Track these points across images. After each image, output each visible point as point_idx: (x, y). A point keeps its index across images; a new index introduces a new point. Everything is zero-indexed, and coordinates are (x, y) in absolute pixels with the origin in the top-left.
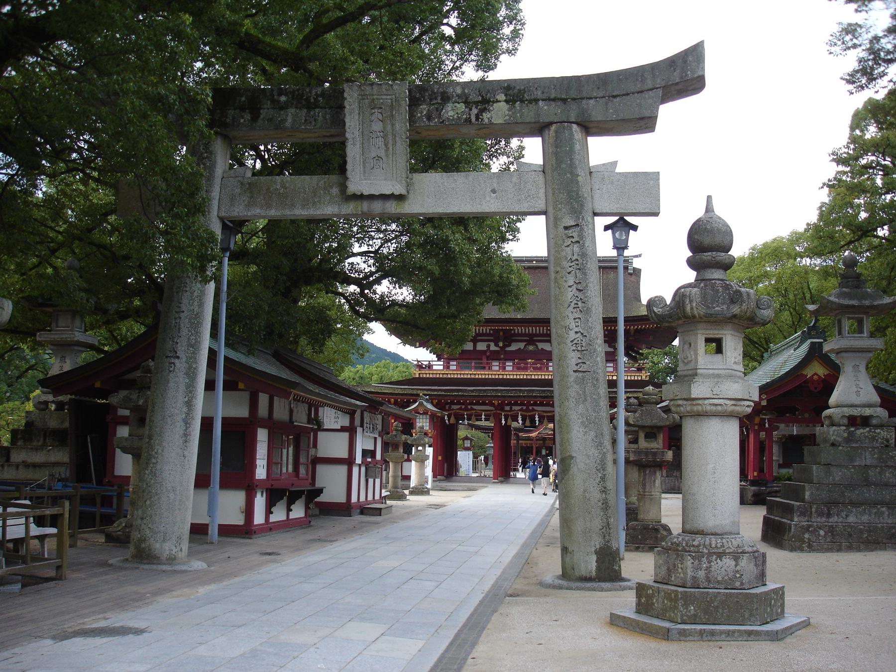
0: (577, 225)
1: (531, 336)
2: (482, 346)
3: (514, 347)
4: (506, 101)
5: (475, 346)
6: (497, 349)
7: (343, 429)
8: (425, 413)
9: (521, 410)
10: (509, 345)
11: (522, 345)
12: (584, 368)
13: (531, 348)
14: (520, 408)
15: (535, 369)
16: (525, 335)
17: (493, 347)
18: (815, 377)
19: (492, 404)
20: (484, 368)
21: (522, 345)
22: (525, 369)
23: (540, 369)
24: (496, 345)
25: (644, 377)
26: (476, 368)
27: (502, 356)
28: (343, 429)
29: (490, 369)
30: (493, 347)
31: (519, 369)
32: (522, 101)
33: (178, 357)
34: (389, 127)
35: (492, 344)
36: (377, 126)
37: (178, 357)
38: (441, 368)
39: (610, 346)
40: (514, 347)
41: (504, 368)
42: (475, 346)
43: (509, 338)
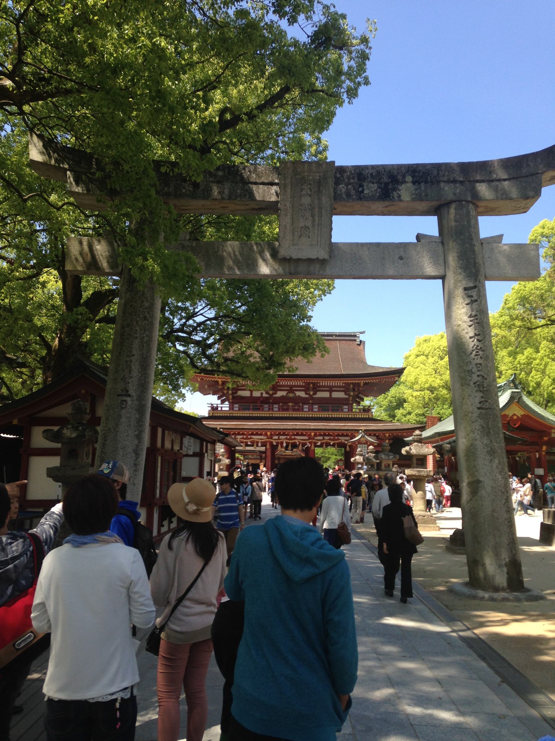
0: (475, 287)
1: (291, 387)
4: (414, 183)
6: (267, 396)
7: (195, 455)
9: (286, 439)
10: (276, 393)
11: (284, 393)
12: (487, 405)
13: (291, 395)
14: (285, 437)
15: (294, 410)
18: (515, 417)
19: (266, 434)
22: (287, 410)
23: (298, 410)
26: (255, 409)
28: (195, 455)
29: (263, 410)
31: (284, 410)
32: (426, 182)
33: (129, 396)
34: (316, 202)
36: (306, 200)
37: (129, 396)
38: (228, 409)
39: (346, 394)
40: (280, 394)
41: (273, 409)
43: (275, 388)
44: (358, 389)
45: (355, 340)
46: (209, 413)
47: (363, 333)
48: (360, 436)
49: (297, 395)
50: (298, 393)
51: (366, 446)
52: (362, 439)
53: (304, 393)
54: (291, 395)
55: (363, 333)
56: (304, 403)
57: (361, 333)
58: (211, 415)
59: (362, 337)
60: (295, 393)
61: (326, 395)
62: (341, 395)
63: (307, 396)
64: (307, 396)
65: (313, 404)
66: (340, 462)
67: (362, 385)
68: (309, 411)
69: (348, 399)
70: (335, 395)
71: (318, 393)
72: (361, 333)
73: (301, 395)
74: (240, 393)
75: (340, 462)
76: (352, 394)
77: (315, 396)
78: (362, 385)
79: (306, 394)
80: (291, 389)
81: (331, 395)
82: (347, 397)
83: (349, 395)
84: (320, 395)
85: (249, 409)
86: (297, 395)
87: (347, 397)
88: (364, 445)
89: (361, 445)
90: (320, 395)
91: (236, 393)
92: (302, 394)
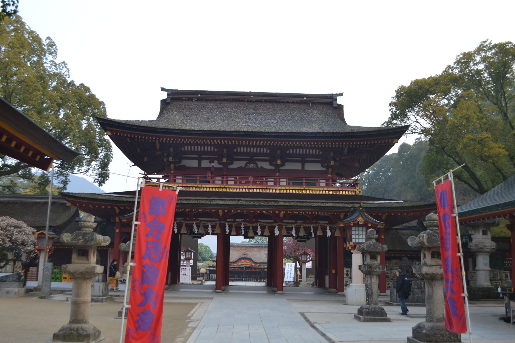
2: (205, 164)
3: (236, 165)
5: (200, 164)
10: (232, 164)
11: (243, 164)
13: (251, 166)
16: (247, 154)
20: (208, 182)
21: (243, 164)
22: (248, 183)
25: (358, 193)
26: (201, 182)
27: (224, 173)
29: (214, 182)
39: (322, 166)
40: (236, 165)
41: (227, 183)
42: (200, 164)
47: (341, 95)
49: (259, 166)
50: (260, 164)
51: (364, 229)
53: (268, 163)
55: (341, 95)
56: (268, 177)
59: (340, 101)
60: (257, 165)
61: (298, 166)
62: (317, 167)
63: (273, 168)
64: (273, 168)
65: (280, 177)
66: (303, 256)
67: (346, 151)
69: (326, 172)
70: (309, 167)
73: (264, 167)
76: (333, 163)
77: (282, 168)
80: (252, 158)
81: (303, 166)
82: (324, 169)
83: (328, 167)
84: (289, 166)
86: (259, 166)
87: (324, 169)
88: (361, 229)
89: (357, 229)
90: (289, 166)
91: (181, 163)
92: (266, 166)
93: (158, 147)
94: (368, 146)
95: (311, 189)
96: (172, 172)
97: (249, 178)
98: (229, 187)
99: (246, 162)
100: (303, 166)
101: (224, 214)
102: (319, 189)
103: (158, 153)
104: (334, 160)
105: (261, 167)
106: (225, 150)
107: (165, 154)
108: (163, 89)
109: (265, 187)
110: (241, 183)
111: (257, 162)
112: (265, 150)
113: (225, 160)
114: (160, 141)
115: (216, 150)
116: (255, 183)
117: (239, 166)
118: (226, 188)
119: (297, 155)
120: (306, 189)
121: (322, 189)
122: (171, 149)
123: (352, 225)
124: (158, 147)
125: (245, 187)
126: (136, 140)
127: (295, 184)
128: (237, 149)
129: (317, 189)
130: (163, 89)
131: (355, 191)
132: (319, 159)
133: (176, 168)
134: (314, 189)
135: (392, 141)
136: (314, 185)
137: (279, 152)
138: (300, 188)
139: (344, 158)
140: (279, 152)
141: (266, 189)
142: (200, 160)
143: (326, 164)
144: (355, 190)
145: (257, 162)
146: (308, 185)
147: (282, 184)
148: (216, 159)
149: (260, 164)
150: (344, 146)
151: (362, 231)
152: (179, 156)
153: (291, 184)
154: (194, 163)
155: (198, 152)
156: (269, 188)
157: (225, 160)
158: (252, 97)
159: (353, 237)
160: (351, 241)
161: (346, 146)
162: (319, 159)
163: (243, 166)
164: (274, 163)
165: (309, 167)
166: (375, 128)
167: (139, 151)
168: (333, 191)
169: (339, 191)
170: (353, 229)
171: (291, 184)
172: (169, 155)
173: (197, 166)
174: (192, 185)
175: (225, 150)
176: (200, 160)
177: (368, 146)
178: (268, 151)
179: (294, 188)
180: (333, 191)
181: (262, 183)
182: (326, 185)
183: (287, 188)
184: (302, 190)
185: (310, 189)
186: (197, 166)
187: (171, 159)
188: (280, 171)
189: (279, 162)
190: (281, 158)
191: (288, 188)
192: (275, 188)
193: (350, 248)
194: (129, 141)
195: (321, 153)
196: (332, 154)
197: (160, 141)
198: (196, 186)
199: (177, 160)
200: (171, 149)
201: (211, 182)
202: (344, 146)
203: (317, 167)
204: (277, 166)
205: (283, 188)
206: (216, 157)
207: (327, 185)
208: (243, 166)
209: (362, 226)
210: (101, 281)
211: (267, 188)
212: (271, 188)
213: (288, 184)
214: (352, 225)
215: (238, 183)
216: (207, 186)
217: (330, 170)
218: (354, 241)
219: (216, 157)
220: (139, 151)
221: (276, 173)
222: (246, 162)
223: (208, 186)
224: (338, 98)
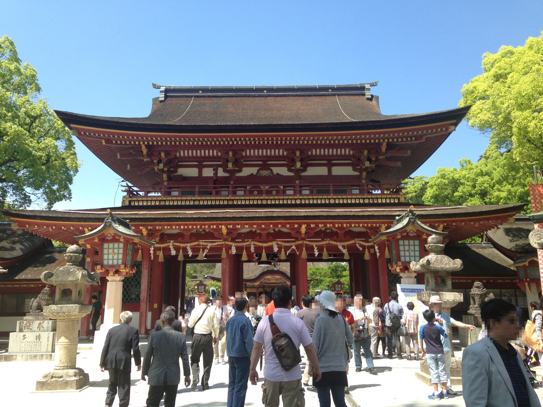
2: (208, 172)
5: (200, 172)
6: (227, 175)
8: (115, 239)
10: (240, 171)
11: (254, 170)
13: (265, 173)
16: (258, 158)
17: (221, 173)
20: (211, 194)
22: (260, 193)
24: (225, 171)
26: (201, 193)
29: (217, 193)
30: (221, 173)
35: (220, 170)
39: (354, 170)
40: (246, 172)
42: (200, 172)
43: (239, 164)
44: (377, 159)
45: (364, 95)
46: (123, 201)
48: (405, 221)
49: (275, 173)
50: (276, 170)
51: (417, 242)
52: (410, 228)
54: (265, 173)
57: (372, 85)
58: (127, 203)
60: (271, 170)
61: (322, 171)
62: (348, 171)
63: (292, 174)
64: (292, 174)
66: (336, 286)
67: (384, 148)
68: (295, 194)
69: (359, 177)
70: (337, 171)
71: (309, 169)
72: (372, 85)
73: (281, 173)
74: (182, 171)
75: (336, 286)
76: (367, 164)
78: (384, 148)
79: (290, 170)
81: (330, 171)
82: (357, 173)
83: (361, 171)
84: (312, 171)
85: (193, 193)
86: (275, 173)
87: (357, 173)
88: (412, 242)
89: (406, 242)
90: (312, 171)
91: (176, 171)
92: (283, 171)
93: (145, 151)
94: (414, 139)
95: (340, 197)
96: (166, 183)
97: (262, 187)
98: (237, 198)
99: (258, 168)
100: (330, 171)
101: (230, 232)
102: (350, 197)
103: (145, 160)
104: (369, 159)
105: (278, 174)
106: (231, 154)
107: (155, 161)
108: (155, 86)
109: (282, 197)
110: (251, 193)
111: (271, 168)
112: (281, 151)
113: (230, 165)
114: (146, 143)
115: (219, 154)
116: (269, 193)
117: (250, 174)
118: (233, 200)
119: (321, 158)
120: (334, 197)
121: (355, 197)
122: (163, 154)
123: (399, 237)
124: (145, 151)
125: (256, 198)
126: (114, 142)
127: (320, 192)
128: (246, 152)
129: (349, 197)
130: (155, 86)
131: (399, 199)
132: (350, 162)
133: (170, 179)
134: (344, 197)
135: (447, 129)
136: (344, 192)
137: (298, 153)
138: (326, 197)
139: (381, 157)
140: (298, 153)
141: (283, 199)
142: (200, 167)
143: (358, 167)
144: (398, 196)
145: (271, 168)
146: (336, 192)
147: (304, 192)
148: (220, 166)
149: (276, 170)
150: (382, 141)
151: (414, 245)
152: (174, 163)
153: (314, 191)
154: (193, 172)
155: (197, 157)
156: (287, 197)
157: (230, 165)
158: (265, 91)
159: (402, 253)
160: (400, 261)
161: (384, 141)
162: (350, 162)
163: (255, 173)
164: (293, 168)
165: (337, 171)
166: (421, 115)
167: (119, 157)
168: (369, 199)
169: (377, 198)
170: (401, 242)
171: (314, 191)
172: (160, 162)
173: (197, 175)
174: (189, 198)
175: (231, 154)
176: (200, 167)
177: (414, 139)
178: (285, 153)
179: (319, 197)
180: (369, 199)
181: (278, 193)
182: (360, 192)
183: (309, 197)
184: (329, 199)
185: (339, 197)
186: (197, 175)
187: (161, 166)
188: (300, 178)
189: (298, 165)
190: (301, 160)
191: (311, 197)
192: (295, 197)
193: (398, 270)
194: (104, 143)
195: (351, 153)
196: (366, 152)
197: (146, 143)
198: (194, 198)
199: (172, 169)
200: (163, 154)
201: (214, 193)
202: (382, 141)
203: (348, 171)
204: (297, 171)
205: (305, 197)
206: (221, 163)
207: (362, 192)
208: (255, 173)
209: (414, 238)
210: (50, 329)
211: (285, 197)
212: (290, 197)
213: (312, 193)
214: (399, 237)
215: (247, 193)
216: (208, 198)
217: (364, 174)
218: (403, 259)
219: (221, 163)
220: (119, 157)
221: (297, 182)
222: (258, 168)
223: (209, 198)
224: (372, 88)
